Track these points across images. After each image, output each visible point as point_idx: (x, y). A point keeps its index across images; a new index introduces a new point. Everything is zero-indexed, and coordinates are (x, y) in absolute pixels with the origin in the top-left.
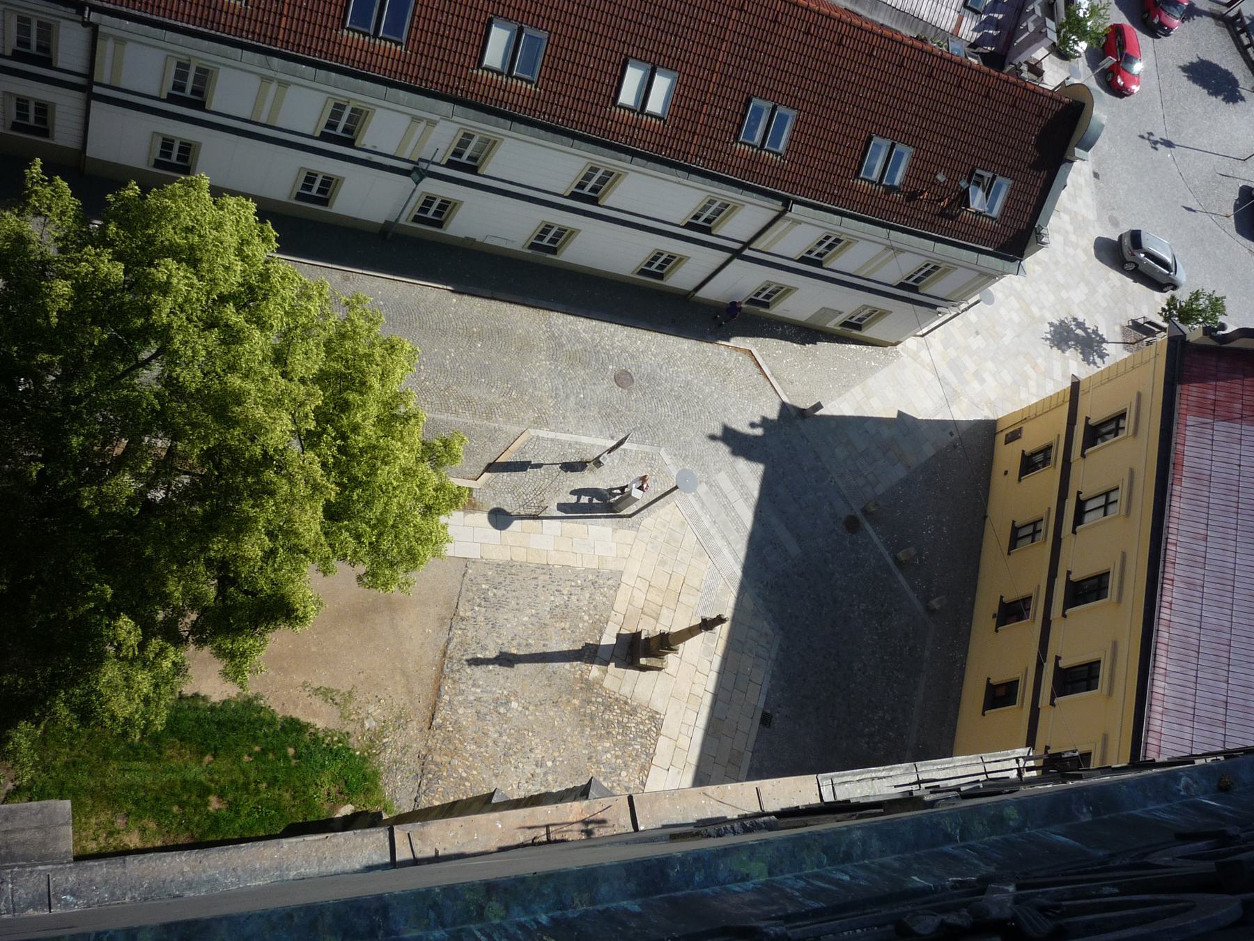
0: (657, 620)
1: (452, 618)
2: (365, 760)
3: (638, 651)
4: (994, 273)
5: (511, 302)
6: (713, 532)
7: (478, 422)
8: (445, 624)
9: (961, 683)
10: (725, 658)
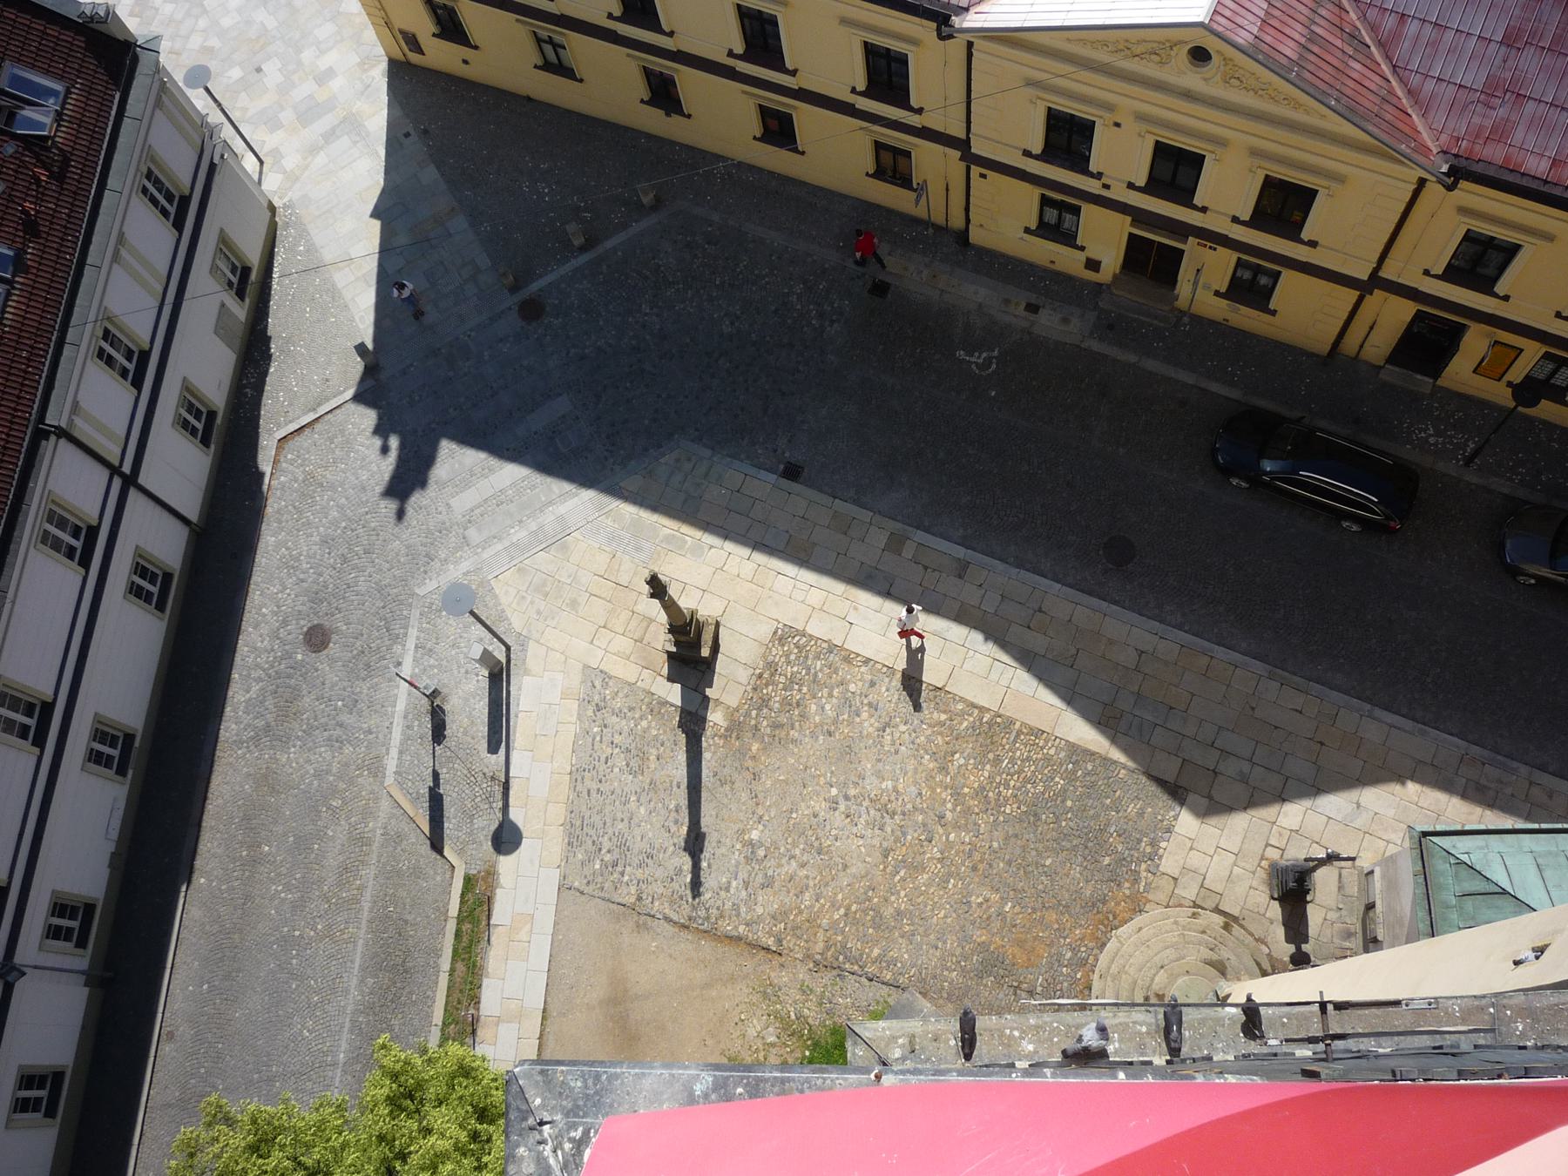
0: (652, 620)
1: (638, 913)
2: (816, 1045)
3: (691, 653)
4: (156, 85)
5: (205, 798)
6: (533, 526)
7: (374, 856)
8: (645, 924)
9: (760, 170)
10: (706, 526)
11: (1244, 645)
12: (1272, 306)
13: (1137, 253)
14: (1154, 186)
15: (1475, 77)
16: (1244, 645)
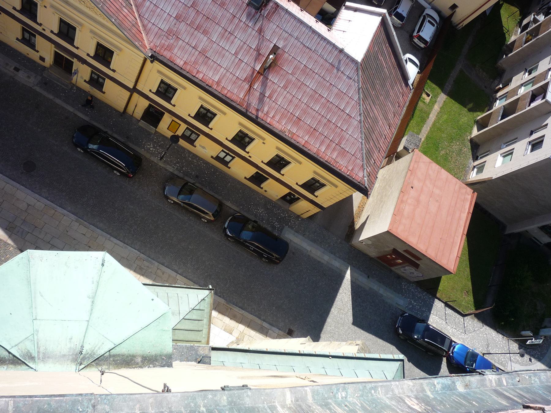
11: (69, 208)
12: (103, 90)
13: (58, 58)
14: (60, 34)
15: (165, 27)
16: (69, 208)
